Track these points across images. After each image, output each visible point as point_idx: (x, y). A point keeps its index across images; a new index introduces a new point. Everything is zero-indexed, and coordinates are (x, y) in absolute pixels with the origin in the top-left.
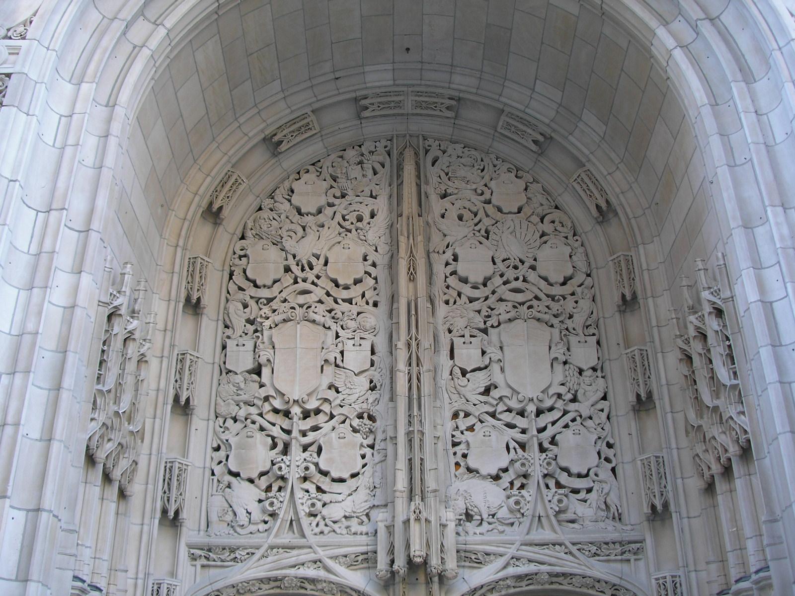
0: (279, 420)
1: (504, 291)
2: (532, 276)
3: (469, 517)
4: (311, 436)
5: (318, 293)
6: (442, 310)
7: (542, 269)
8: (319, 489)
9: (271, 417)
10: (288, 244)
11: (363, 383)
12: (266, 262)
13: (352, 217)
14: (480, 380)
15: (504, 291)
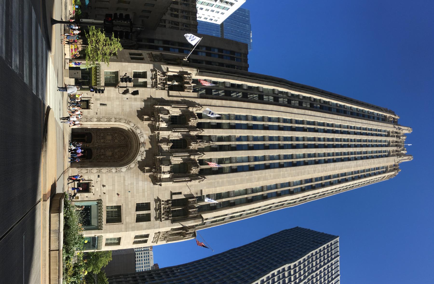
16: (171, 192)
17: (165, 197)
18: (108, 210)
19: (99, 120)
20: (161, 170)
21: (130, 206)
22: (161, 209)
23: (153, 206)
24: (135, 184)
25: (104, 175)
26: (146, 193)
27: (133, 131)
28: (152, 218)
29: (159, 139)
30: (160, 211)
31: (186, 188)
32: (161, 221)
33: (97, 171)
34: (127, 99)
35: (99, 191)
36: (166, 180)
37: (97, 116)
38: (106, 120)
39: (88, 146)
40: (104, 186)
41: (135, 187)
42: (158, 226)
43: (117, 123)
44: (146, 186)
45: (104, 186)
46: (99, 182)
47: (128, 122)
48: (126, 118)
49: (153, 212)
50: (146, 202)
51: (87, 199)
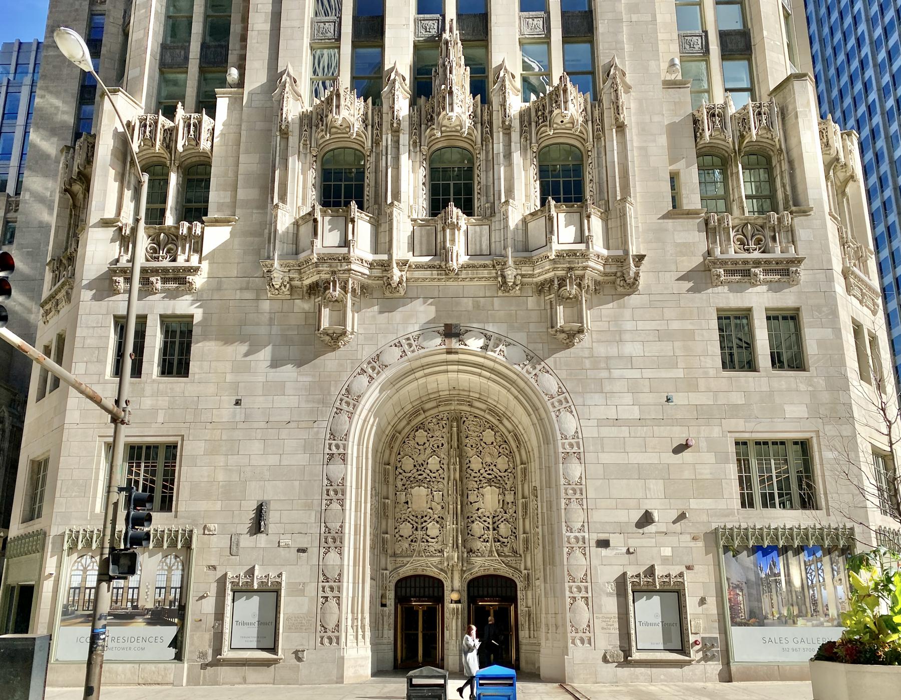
0: (414, 518)
1: (485, 475)
2: (495, 469)
3: (471, 551)
4: (424, 524)
5: (425, 475)
6: (465, 481)
7: (499, 466)
8: (427, 541)
9: (411, 517)
10: (414, 457)
11: (439, 507)
12: (408, 464)
13: (436, 446)
14: (476, 506)
15: (485, 475)
16: (666, 216)
17: (691, 241)
18: (758, 499)
19: (332, 539)
20: (573, 253)
21: (737, 399)
22: (746, 262)
23: (726, 297)
24: (635, 374)
25: (597, 516)
26: (675, 325)
27: (393, 382)
28: (786, 299)
29: (431, 267)
30: (757, 263)
31: (646, 150)
32: (799, 261)
33: (578, 553)
34: (238, 403)
35: (673, 540)
36: (616, 229)
37: (314, 551)
38: (335, 506)
39: (455, 596)
40: (646, 519)
41: (648, 373)
42: (821, 276)
43: (352, 451)
44: (641, 325)
45: (646, 519)
46: (633, 543)
47: (351, 398)
48: (330, 411)
49: (759, 299)
50: (714, 324)
51: (712, 601)
